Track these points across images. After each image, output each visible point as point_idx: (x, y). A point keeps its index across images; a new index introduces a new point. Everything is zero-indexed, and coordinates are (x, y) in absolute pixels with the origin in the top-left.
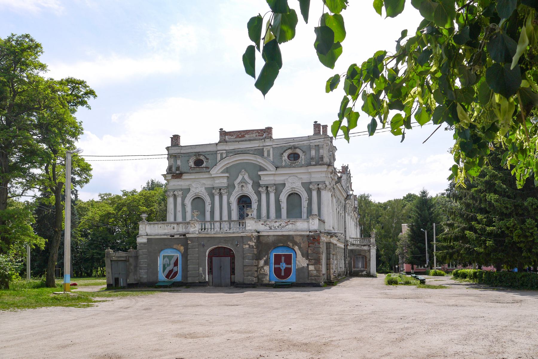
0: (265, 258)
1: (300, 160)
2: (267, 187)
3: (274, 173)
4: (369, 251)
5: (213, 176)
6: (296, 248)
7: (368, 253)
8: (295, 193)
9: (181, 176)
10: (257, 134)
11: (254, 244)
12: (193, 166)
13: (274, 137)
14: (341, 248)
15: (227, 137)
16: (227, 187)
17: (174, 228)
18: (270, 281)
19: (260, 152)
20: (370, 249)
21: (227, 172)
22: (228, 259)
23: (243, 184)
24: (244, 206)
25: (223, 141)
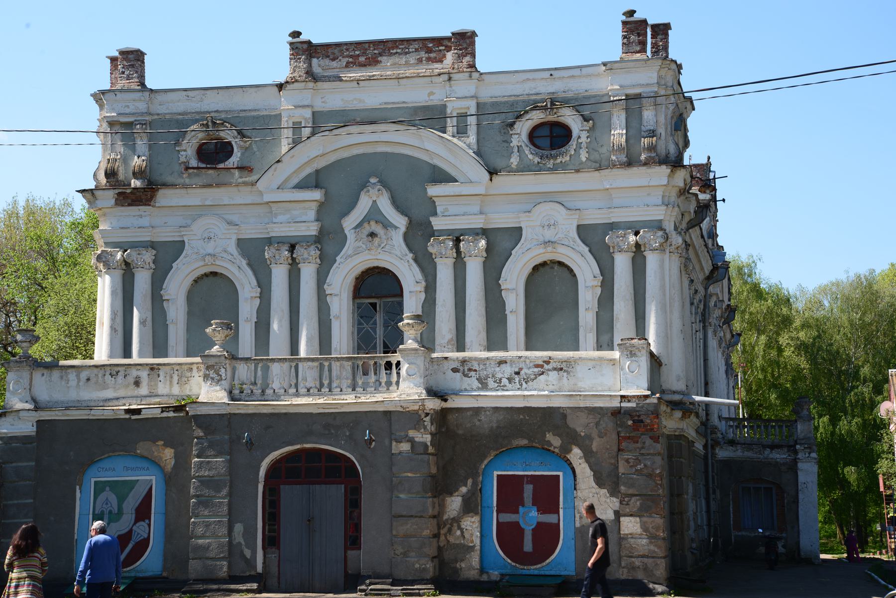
0: (464, 490)
2: (457, 241)
3: (481, 190)
4: (793, 467)
5: (267, 198)
6: (576, 455)
8: (553, 262)
10: (423, 54)
11: (428, 438)
12: (194, 163)
13: (482, 65)
15: (315, 61)
16: (318, 240)
17: (137, 383)
18: (482, 571)
19: (432, 117)
20: (795, 461)
21: (317, 186)
22: (336, 492)
24: (374, 305)
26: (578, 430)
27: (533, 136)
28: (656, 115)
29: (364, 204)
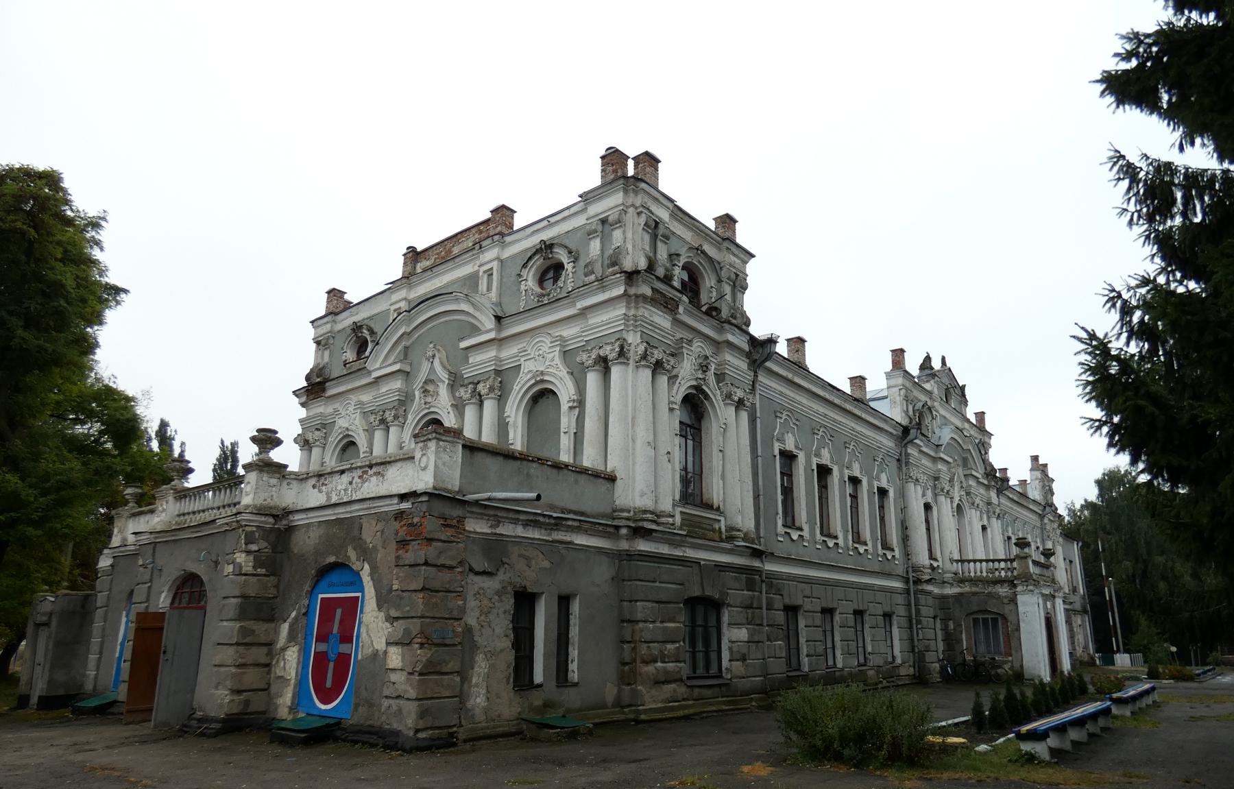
0: (293, 614)
1: (560, 283)
3: (492, 335)
5: (375, 375)
7: (1011, 607)
9: (324, 390)
10: (477, 236)
14: (891, 591)
16: (401, 403)
23: (430, 388)
25: (408, 278)
26: (368, 541)
27: (541, 282)
28: (624, 232)
29: (425, 366)
